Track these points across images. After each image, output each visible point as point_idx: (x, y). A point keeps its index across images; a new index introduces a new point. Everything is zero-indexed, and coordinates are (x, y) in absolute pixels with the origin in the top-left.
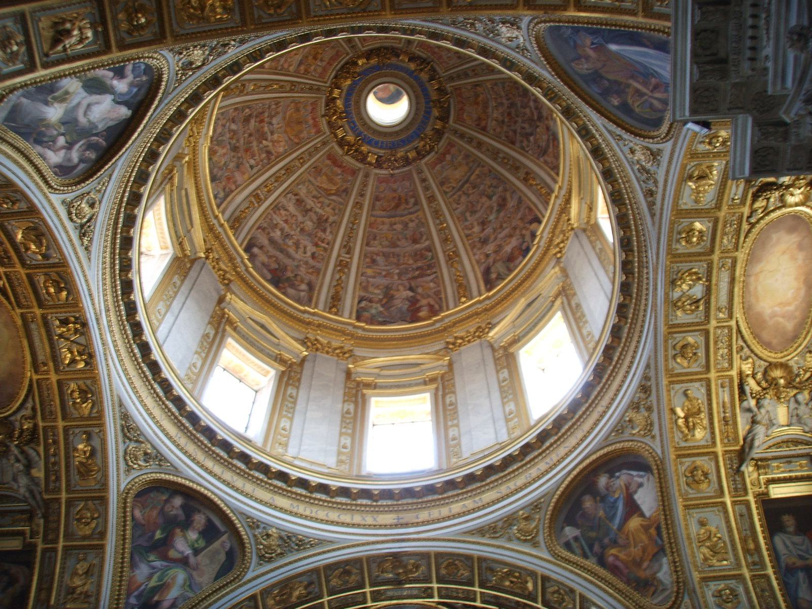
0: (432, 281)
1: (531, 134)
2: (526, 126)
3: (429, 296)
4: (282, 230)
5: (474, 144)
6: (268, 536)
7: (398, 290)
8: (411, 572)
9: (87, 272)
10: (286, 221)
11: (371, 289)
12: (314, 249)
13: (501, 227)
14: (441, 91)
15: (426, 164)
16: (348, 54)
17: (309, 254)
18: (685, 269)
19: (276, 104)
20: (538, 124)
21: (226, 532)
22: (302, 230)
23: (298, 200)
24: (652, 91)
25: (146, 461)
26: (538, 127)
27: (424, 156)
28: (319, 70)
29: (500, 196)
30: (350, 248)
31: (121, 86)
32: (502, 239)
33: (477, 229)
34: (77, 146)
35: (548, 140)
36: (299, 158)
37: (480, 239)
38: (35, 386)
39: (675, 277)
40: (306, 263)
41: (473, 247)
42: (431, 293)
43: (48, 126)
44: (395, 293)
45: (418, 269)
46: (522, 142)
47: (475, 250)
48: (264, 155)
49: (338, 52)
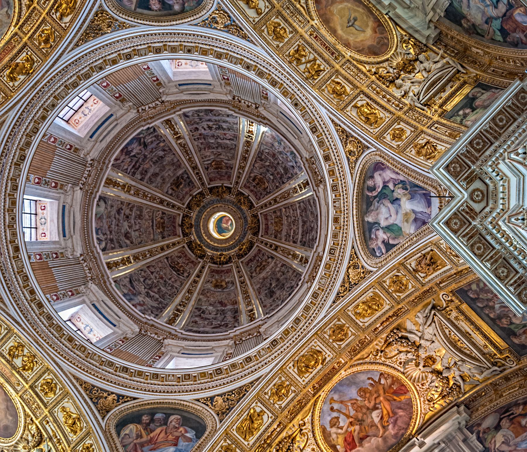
0: (127, 169)
1: (144, 281)
2: (150, 282)
3: (123, 162)
4: (224, 129)
5: (165, 248)
6: (110, 26)
7: (140, 150)
8: (11, 73)
9: (326, 110)
10: (225, 134)
11: (154, 139)
12: (199, 132)
13: (118, 225)
14: (202, 257)
15: (180, 215)
16: (262, 236)
17: (200, 128)
18: (35, 368)
19: (277, 186)
20: (146, 290)
21: (135, 9)
22: (213, 136)
23: (228, 147)
24: (135, 444)
25: (214, 18)
26: (145, 288)
27: (183, 217)
28: (269, 217)
29: (131, 237)
30: (181, 146)
31: (382, 235)
32: (112, 221)
33: (128, 212)
34: (381, 186)
35: (134, 289)
36: (244, 167)
37: (122, 210)
38: (309, 18)
39: (36, 360)
40: (198, 124)
41: (122, 203)
42: (122, 165)
43: (405, 195)
44: (140, 147)
45: (139, 166)
46: (145, 272)
47: (120, 203)
48: (263, 157)
49: (268, 234)
